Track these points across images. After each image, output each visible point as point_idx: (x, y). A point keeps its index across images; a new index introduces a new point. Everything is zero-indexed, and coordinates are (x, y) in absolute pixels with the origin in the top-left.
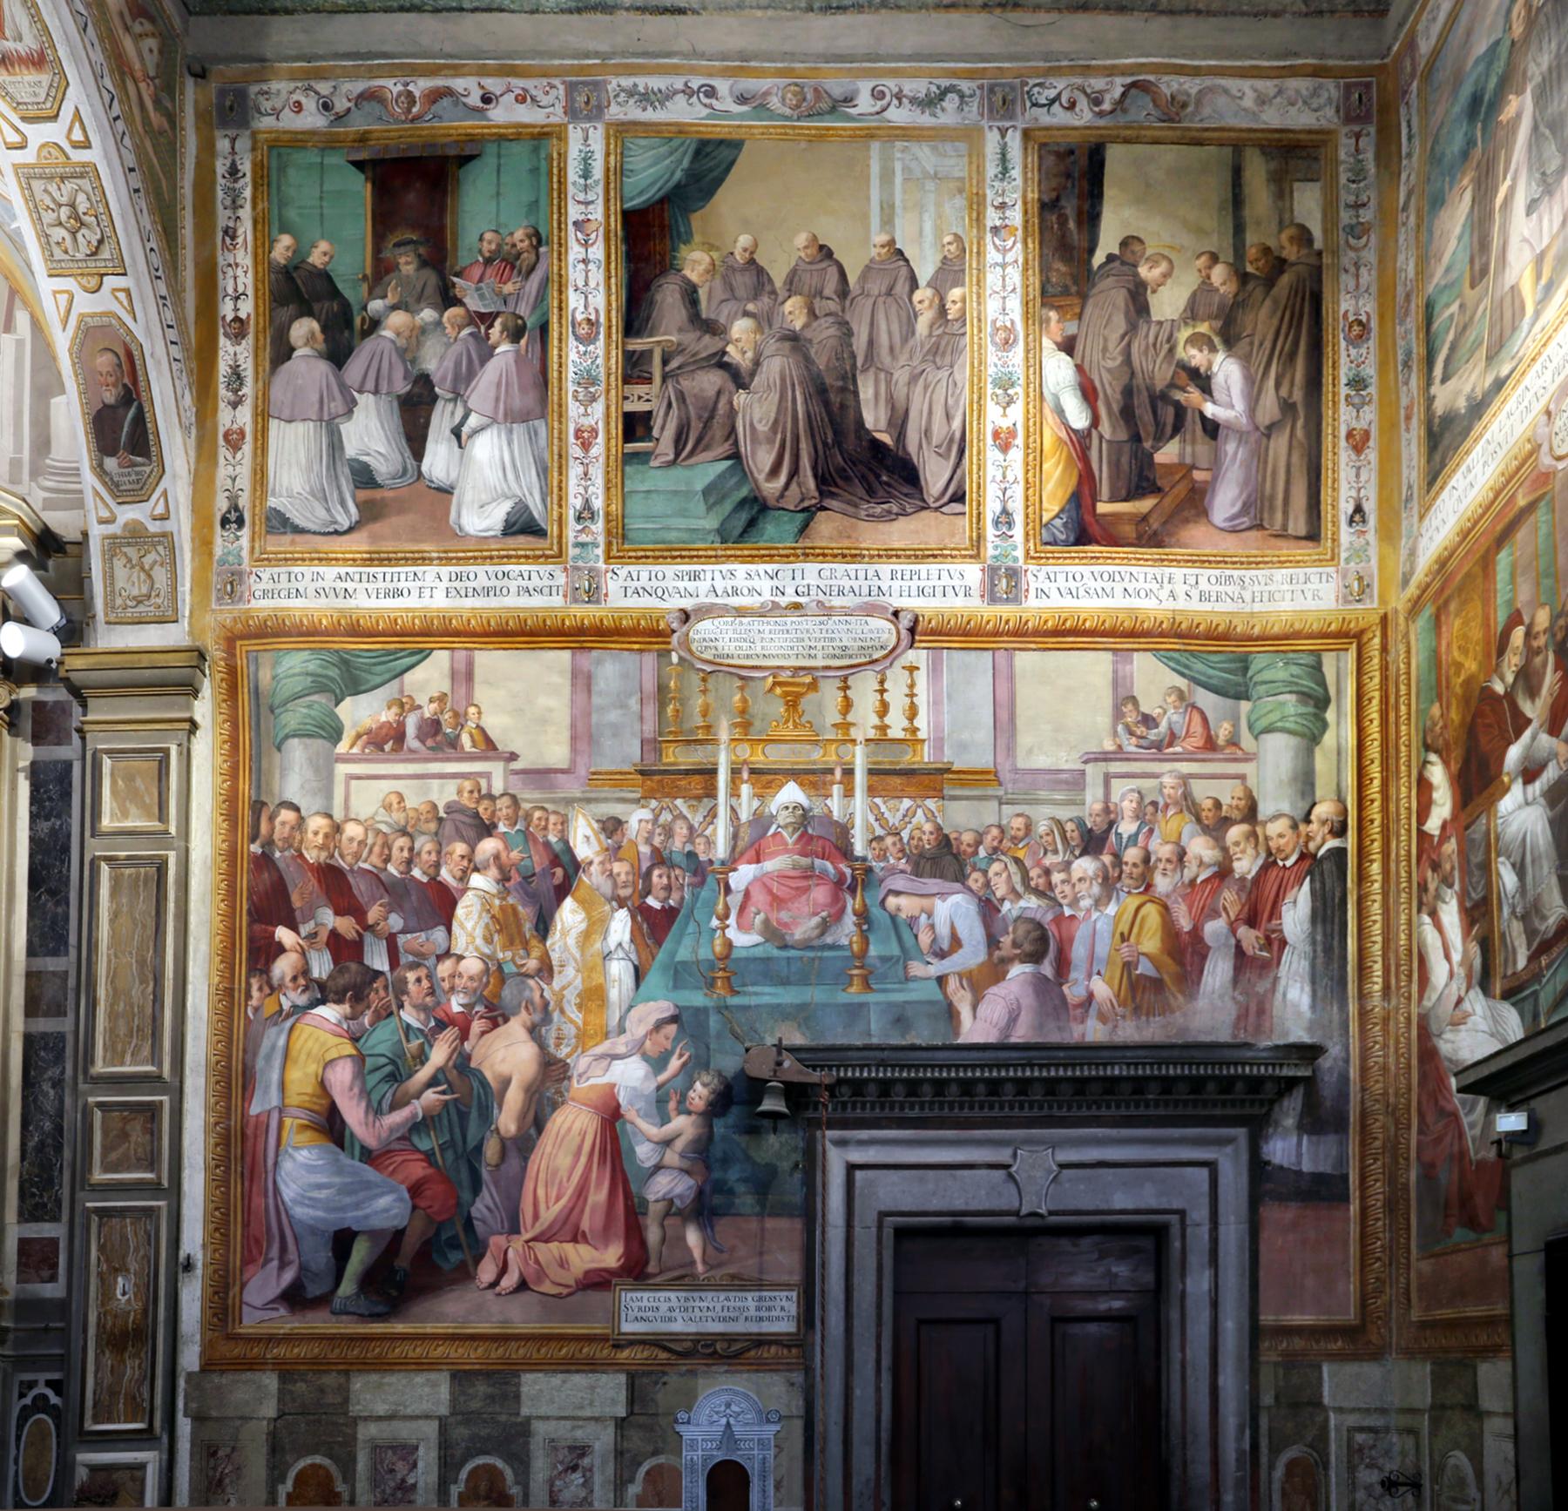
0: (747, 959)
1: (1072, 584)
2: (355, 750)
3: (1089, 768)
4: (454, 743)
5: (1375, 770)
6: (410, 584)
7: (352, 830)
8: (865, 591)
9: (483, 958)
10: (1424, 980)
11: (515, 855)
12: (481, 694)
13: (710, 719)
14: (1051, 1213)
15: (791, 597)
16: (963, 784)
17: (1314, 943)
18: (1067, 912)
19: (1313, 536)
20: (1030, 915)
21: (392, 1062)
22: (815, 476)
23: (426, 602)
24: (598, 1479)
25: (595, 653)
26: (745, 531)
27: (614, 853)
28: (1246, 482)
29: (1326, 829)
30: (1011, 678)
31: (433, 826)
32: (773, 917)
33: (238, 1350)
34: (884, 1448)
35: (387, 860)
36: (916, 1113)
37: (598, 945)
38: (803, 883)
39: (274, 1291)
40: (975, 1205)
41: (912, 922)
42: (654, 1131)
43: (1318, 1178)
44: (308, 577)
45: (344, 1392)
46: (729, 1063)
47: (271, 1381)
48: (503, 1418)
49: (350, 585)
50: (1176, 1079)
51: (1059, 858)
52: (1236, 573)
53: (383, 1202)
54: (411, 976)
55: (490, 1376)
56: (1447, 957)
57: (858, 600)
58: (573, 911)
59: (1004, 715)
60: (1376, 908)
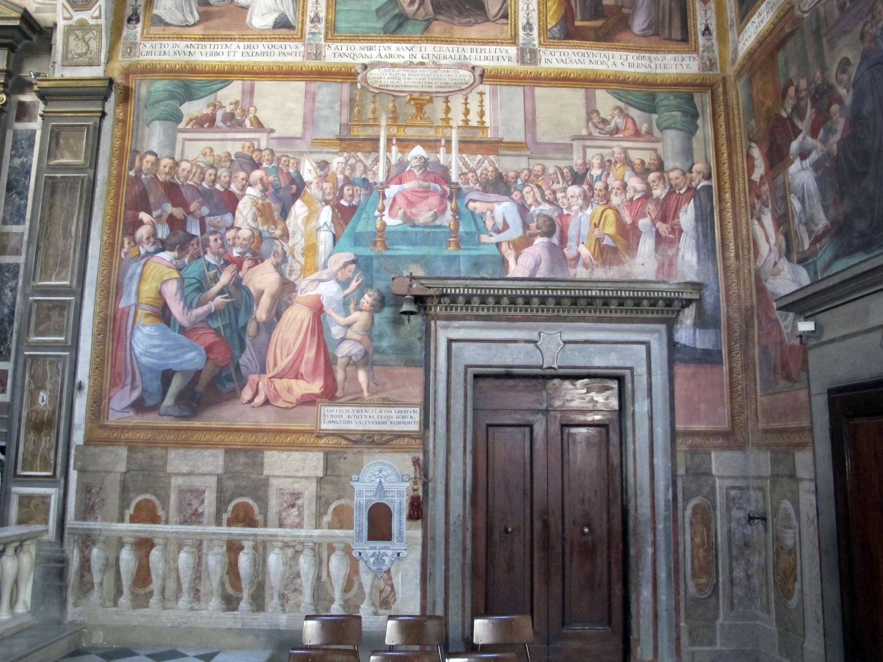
0: (394, 232)
1: (564, 58)
2: (188, 127)
3: (575, 143)
4: (241, 124)
5: (724, 149)
7: (185, 165)
8: (457, 57)
9: (252, 229)
10: (757, 252)
11: (271, 178)
12: (257, 101)
13: (376, 115)
14: (560, 367)
15: (419, 59)
16: (509, 148)
17: (697, 231)
18: (565, 212)
19: (685, 39)
20: (545, 213)
21: (199, 281)
22: (433, 5)
24: (306, 512)
25: (318, 83)
27: (324, 178)
28: (650, 14)
29: (701, 176)
30: (533, 98)
31: (228, 164)
32: (408, 211)
33: (105, 434)
34: (468, 497)
35: (203, 179)
36: (485, 312)
37: (314, 224)
38: (425, 195)
39: (128, 401)
40: (517, 363)
41: (482, 215)
43: (706, 352)
45: (165, 458)
46: (381, 285)
47: (123, 452)
48: (253, 476)
49: (192, 50)
50: (626, 298)
51: (560, 186)
52: (647, 55)
54: (212, 238)
55: (247, 450)
56: (768, 241)
57: (453, 61)
59: (530, 117)
60: (729, 216)
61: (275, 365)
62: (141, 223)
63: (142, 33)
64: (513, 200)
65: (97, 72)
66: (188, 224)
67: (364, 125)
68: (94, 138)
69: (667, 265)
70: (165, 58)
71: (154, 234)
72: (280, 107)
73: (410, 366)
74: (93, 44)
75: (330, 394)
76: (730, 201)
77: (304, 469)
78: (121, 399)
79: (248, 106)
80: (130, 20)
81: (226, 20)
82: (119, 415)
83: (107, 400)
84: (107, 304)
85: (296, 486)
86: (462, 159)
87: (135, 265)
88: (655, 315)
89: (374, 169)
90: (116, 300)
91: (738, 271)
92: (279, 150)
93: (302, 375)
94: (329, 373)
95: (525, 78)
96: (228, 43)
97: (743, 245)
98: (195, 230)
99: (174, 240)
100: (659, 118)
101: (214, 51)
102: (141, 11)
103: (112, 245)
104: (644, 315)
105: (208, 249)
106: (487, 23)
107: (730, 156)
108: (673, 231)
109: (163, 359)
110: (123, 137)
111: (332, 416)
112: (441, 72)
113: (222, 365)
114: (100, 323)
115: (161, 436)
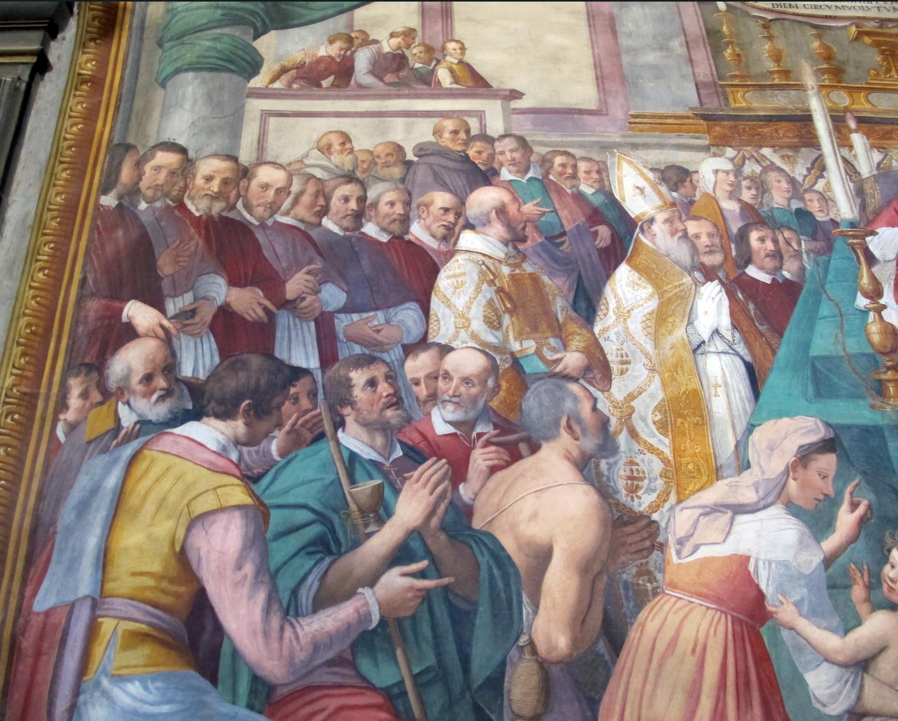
2: (277, 85)
9: (485, 349)
11: (529, 208)
21: (322, 518)
31: (397, 171)
35: (325, 211)
37: (680, 332)
42: (831, 641)
54: (359, 377)
58: (634, 284)
62: (129, 333)
92: (543, 140)
98: (301, 353)
99: (232, 383)
105: (347, 411)
110: (90, 116)
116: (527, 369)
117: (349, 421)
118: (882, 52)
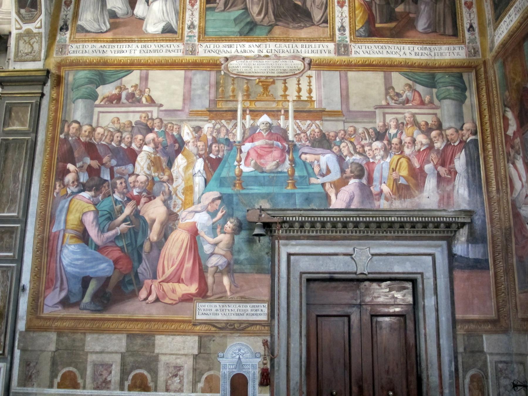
0: (248, 177)
2: (102, 103)
3: (377, 111)
4: (139, 101)
5: (486, 112)
6: (127, 49)
7: (99, 130)
8: (292, 51)
9: (147, 175)
11: (160, 139)
12: (150, 84)
14: (369, 273)
15: (265, 53)
16: (330, 116)
17: (468, 173)
18: (371, 161)
19: (455, 34)
21: (109, 213)
22: (274, 15)
23: (132, 55)
24: (185, 380)
25: (193, 71)
26: (247, 33)
27: (198, 139)
29: (469, 132)
30: (347, 81)
31: (130, 129)
32: (258, 162)
33: (40, 323)
34: (303, 369)
35: (112, 140)
37: (191, 171)
39: (57, 300)
40: (338, 270)
43: (476, 261)
44: (90, 46)
45: (83, 341)
46: (240, 214)
47: (53, 336)
48: (147, 354)
49: (105, 49)
50: (417, 222)
51: (367, 142)
52: (428, 47)
53: (103, 266)
54: (118, 182)
55: (142, 336)
56: (521, 179)
57: (289, 54)
58: (182, 159)
59: (344, 93)
61: (164, 272)
62: (69, 171)
63: (70, 38)
64: (333, 152)
65: (38, 65)
66: (102, 171)
67: (227, 101)
68: (35, 112)
69: (446, 198)
70: (86, 55)
71: (78, 180)
72: (167, 89)
73: (260, 273)
74: (36, 46)
75: (203, 294)
76: (491, 150)
77: (184, 348)
78: (53, 297)
79: (144, 87)
80: (61, 29)
81: (128, 28)
82: (51, 309)
83: (42, 298)
84: (44, 229)
85: (178, 361)
86: (296, 124)
87: (63, 201)
88: (438, 235)
89: (234, 132)
90: (50, 226)
91: (499, 201)
92: (166, 119)
93: (182, 280)
94: (202, 279)
95: (340, 65)
96: (130, 44)
97: (502, 182)
98: (106, 176)
99: (91, 183)
100: (437, 92)
101: (120, 49)
102: (69, 23)
103: (48, 187)
104: (430, 235)
105: (116, 190)
106: (313, 27)
107: (490, 117)
108: (450, 173)
109: (84, 269)
110: (56, 111)
111: (204, 310)
112: (280, 62)
113: (125, 273)
114: (38, 243)
115: (81, 325)
116: (155, 180)
117: (116, 192)
118: (264, 88)
